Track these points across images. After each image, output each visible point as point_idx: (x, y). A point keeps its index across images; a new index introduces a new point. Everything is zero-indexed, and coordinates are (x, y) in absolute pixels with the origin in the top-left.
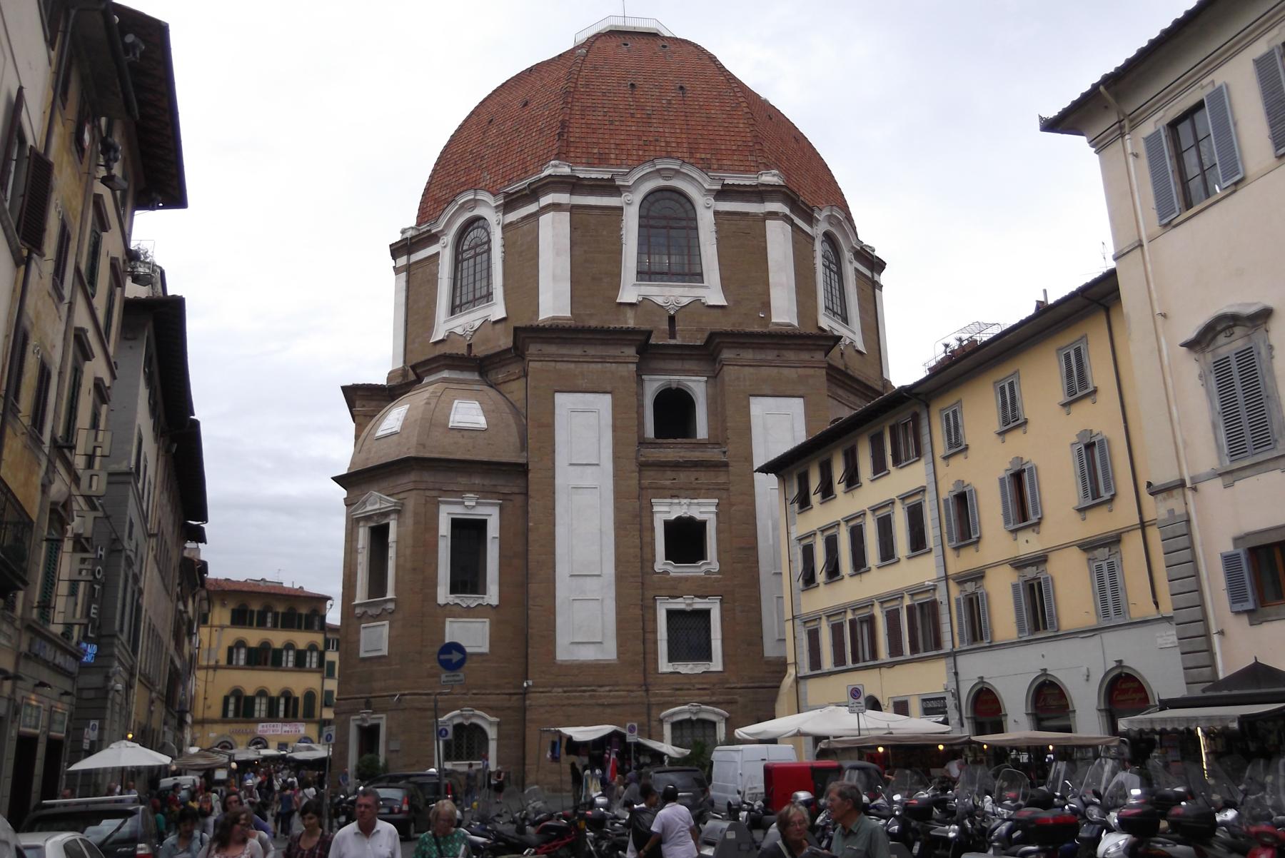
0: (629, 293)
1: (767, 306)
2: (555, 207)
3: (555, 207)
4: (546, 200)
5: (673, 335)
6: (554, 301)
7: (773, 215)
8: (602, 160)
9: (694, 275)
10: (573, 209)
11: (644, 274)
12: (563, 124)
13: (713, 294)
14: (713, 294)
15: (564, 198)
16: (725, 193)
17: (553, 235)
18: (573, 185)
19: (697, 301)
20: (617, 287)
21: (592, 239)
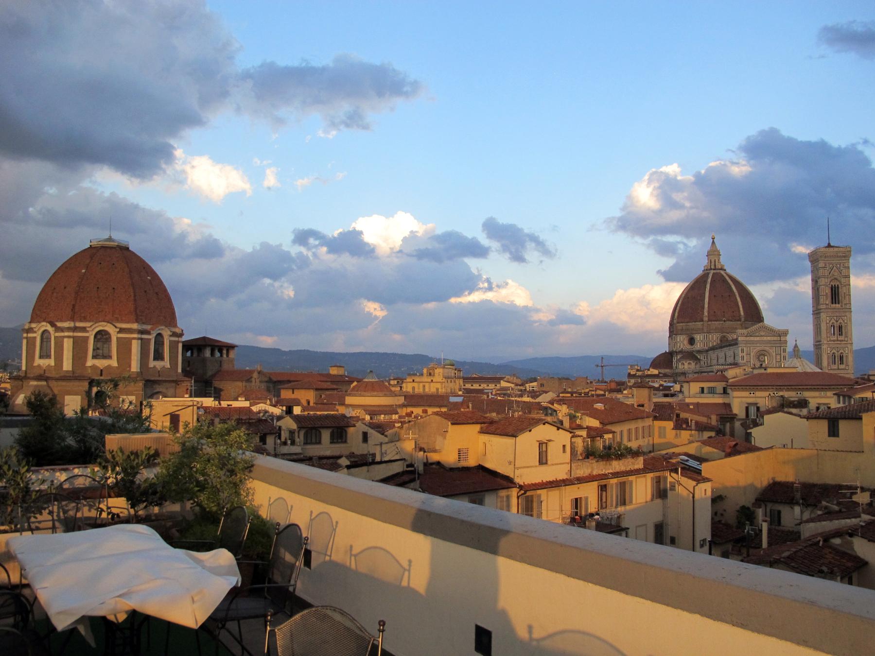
0: (90, 362)
1: (130, 366)
2: (69, 337)
3: (69, 337)
4: (66, 334)
5: (101, 375)
6: (67, 365)
7: (134, 338)
8: (84, 319)
9: (110, 357)
10: (73, 337)
11: (95, 357)
12: (74, 306)
13: (114, 363)
14: (114, 363)
15: (71, 334)
16: (121, 330)
17: (68, 345)
18: (75, 329)
19: (109, 367)
20: (85, 361)
21: (79, 346)
